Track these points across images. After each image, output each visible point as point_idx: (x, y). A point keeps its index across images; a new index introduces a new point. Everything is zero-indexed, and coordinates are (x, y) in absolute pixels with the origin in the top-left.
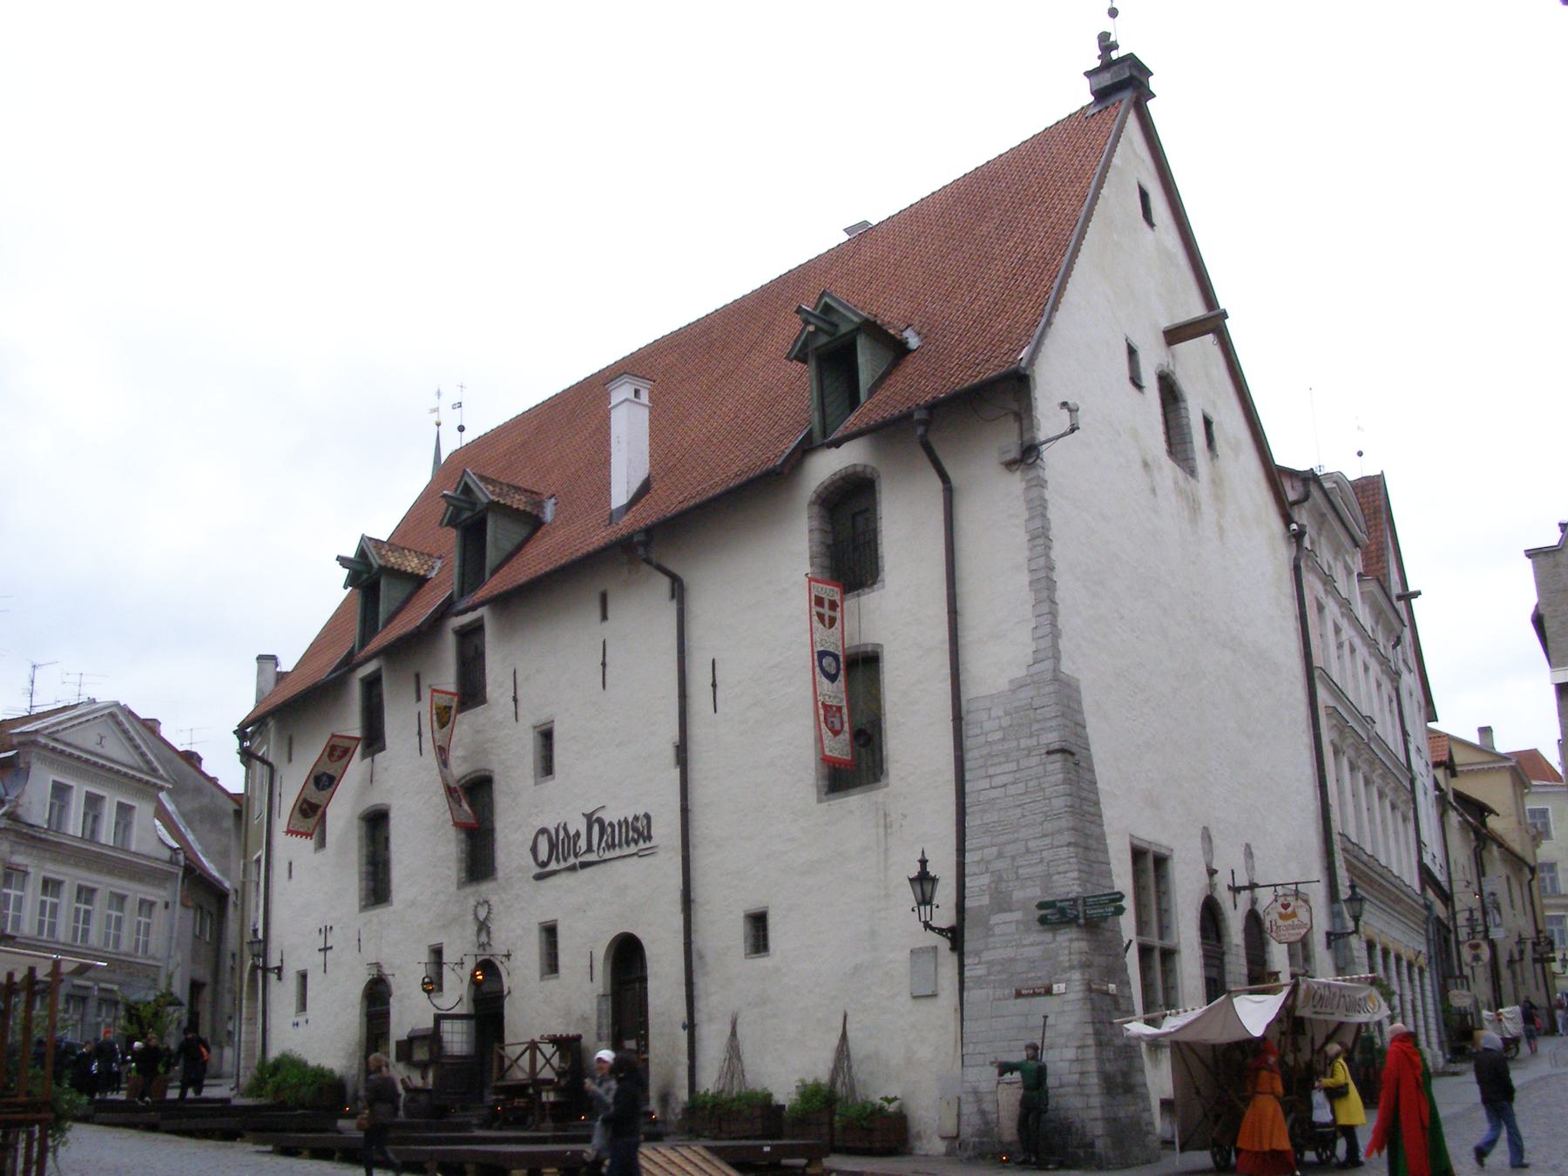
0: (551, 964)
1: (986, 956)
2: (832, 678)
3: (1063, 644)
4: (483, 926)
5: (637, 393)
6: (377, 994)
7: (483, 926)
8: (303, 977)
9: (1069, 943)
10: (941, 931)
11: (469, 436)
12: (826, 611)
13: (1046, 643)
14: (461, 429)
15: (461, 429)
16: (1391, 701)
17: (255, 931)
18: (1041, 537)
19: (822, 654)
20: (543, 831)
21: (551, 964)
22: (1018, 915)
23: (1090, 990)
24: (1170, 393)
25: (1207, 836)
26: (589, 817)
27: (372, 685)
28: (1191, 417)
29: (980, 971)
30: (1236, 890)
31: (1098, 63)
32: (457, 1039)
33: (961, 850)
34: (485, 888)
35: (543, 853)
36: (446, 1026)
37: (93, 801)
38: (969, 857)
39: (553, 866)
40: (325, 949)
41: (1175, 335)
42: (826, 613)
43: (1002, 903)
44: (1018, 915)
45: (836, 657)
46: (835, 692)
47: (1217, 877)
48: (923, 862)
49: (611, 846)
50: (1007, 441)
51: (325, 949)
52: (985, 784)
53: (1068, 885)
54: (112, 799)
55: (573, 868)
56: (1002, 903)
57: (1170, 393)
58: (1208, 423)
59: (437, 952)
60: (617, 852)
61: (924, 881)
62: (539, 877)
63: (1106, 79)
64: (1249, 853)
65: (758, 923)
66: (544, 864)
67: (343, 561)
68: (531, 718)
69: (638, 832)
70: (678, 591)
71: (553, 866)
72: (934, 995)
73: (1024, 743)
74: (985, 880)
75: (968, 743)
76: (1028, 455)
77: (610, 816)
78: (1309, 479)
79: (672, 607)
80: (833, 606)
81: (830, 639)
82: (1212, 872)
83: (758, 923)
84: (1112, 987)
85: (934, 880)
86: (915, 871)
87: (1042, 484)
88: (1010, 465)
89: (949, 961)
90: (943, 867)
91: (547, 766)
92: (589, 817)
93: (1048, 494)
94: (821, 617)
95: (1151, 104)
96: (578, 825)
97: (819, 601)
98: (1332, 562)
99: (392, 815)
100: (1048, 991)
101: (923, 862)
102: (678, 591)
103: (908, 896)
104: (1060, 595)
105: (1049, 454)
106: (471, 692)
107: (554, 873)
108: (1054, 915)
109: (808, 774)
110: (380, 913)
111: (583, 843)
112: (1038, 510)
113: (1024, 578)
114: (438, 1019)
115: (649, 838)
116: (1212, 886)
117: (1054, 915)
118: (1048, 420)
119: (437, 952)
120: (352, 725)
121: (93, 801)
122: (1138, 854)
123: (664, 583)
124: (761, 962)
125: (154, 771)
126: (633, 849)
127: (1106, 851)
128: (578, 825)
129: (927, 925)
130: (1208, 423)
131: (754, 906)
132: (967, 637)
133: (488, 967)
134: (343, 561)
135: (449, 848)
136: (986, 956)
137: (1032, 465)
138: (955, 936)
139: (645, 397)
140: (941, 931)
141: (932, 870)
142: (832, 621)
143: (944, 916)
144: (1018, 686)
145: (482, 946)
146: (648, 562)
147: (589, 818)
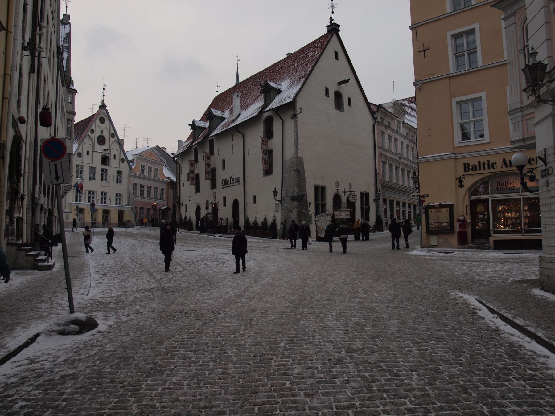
0: (225, 205)
1: (284, 205)
2: (266, 155)
3: (299, 151)
4: (215, 197)
5: (238, 96)
6: (198, 209)
7: (215, 197)
8: (186, 205)
9: (296, 204)
10: (278, 201)
11: (219, 93)
12: (264, 143)
13: (296, 151)
14: (217, 91)
15: (217, 91)
16: (413, 148)
17: (177, 197)
18: (296, 132)
19: (264, 150)
20: (223, 179)
21: (225, 205)
22: (289, 198)
23: (298, 211)
24: (338, 96)
25: (337, 183)
26: (230, 177)
27: (196, 149)
28: (344, 99)
29: (283, 208)
30: (345, 192)
31: (329, 24)
32: (210, 216)
33: (282, 187)
34: (214, 190)
35: (223, 184)
36: (208, 215)
37: (150, 168)
38: (283, 188)
39: (225, 186)
40: (190, 200)
41: (340, 83)
42: (264, 142)
43: (287, 196)
44: (289, 198)
45: (266, 151)
46: (266, 157)
47: (339, 191)
48: (275, 189)
49: (234, 183)
50: (292, 113)
51: (190, 200)
52: (286, 175)
53: (296, 193)
54: (154, 167)
55: (228, 187)
56: (287, 196)
57: (338, 96)
58: (349, 100)
59: (208, 201)
60: (234, 184)
61: (275, 193)
62: (223, 188)
63: (330, 28)
64: (350, 185)
65: (255, 197)
66: (224, 186)
67: (189, 125)
68: (221, 158)
69: (237, 180)
70: (244, 137)
71: (225, 186)
72: (278, 211)
73: (292, 168)
74: (285, 192)
75: (284, 168)
76: (294, 116)
77: (234, 177)
78: (380, 106)
79: (242, 139)
80: (266, 141)
81: (265, 148)
82: (338, 190)
83: (255, 197)
84: (304, 211)
85: (277, 192)
86: (274, 190)
87: (297, 122)
88: (292, 118)
89: (280, 204)
90: (279, 190)
91: (224, 168)
92: (230, 177)
93: (298, 124)
94: (263, 144)
95: (339, 33)
96: (229, 179)
97: (263, 141)
98: (390, 121)
99: (200, 175)
100: (292, 211)
101: (275, 189)
102: (244, 137)
103: (273, 195)
104: (299, 142)
105: (298, 116)
106: (212, 152)
107: (225, 187)
108: (293, 199)
109: (262, 172)
110: (199, 194)
111: (229, 182)
112: (296, 127)
113: (293, 139)
114: (207, 214)
115: (239, 182)
116: (338, 192)
117: (293, 199)
118: (298, 111)
119: (208, 201)
120: (192, 158)
121: (150, 168)
122: (317, 188)
123: (242, 135)
124: (255, 205)
125: (162, 161)
126: (237, 184)
127: (306, 187)
128: (229, 179)
129: (276, 200)
130: (349, 100)
131: (254, 195)
132: (285, 149)
133: (216, 204)
134: (189, 125)
135: (209, 182)
136: (284, 205)
137: (295, 118)
138: (281, 201)
139: (240, 96)
140: (278, 201)
141: (277, 190)
142: (266, 144)
143: (279, 198)
144: (292, 158)
145: (215, 200)
146: (237, 131)
147: (231, 178)
